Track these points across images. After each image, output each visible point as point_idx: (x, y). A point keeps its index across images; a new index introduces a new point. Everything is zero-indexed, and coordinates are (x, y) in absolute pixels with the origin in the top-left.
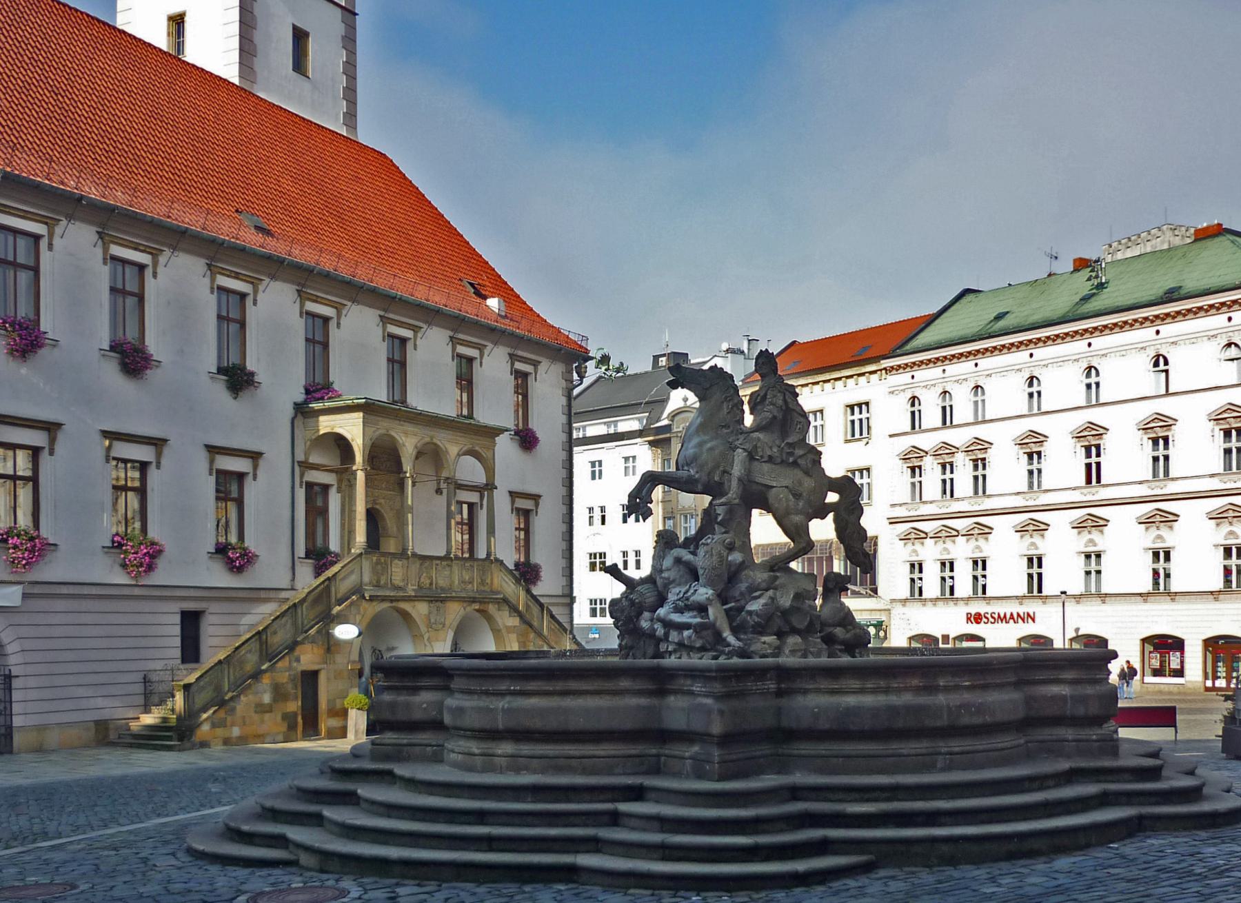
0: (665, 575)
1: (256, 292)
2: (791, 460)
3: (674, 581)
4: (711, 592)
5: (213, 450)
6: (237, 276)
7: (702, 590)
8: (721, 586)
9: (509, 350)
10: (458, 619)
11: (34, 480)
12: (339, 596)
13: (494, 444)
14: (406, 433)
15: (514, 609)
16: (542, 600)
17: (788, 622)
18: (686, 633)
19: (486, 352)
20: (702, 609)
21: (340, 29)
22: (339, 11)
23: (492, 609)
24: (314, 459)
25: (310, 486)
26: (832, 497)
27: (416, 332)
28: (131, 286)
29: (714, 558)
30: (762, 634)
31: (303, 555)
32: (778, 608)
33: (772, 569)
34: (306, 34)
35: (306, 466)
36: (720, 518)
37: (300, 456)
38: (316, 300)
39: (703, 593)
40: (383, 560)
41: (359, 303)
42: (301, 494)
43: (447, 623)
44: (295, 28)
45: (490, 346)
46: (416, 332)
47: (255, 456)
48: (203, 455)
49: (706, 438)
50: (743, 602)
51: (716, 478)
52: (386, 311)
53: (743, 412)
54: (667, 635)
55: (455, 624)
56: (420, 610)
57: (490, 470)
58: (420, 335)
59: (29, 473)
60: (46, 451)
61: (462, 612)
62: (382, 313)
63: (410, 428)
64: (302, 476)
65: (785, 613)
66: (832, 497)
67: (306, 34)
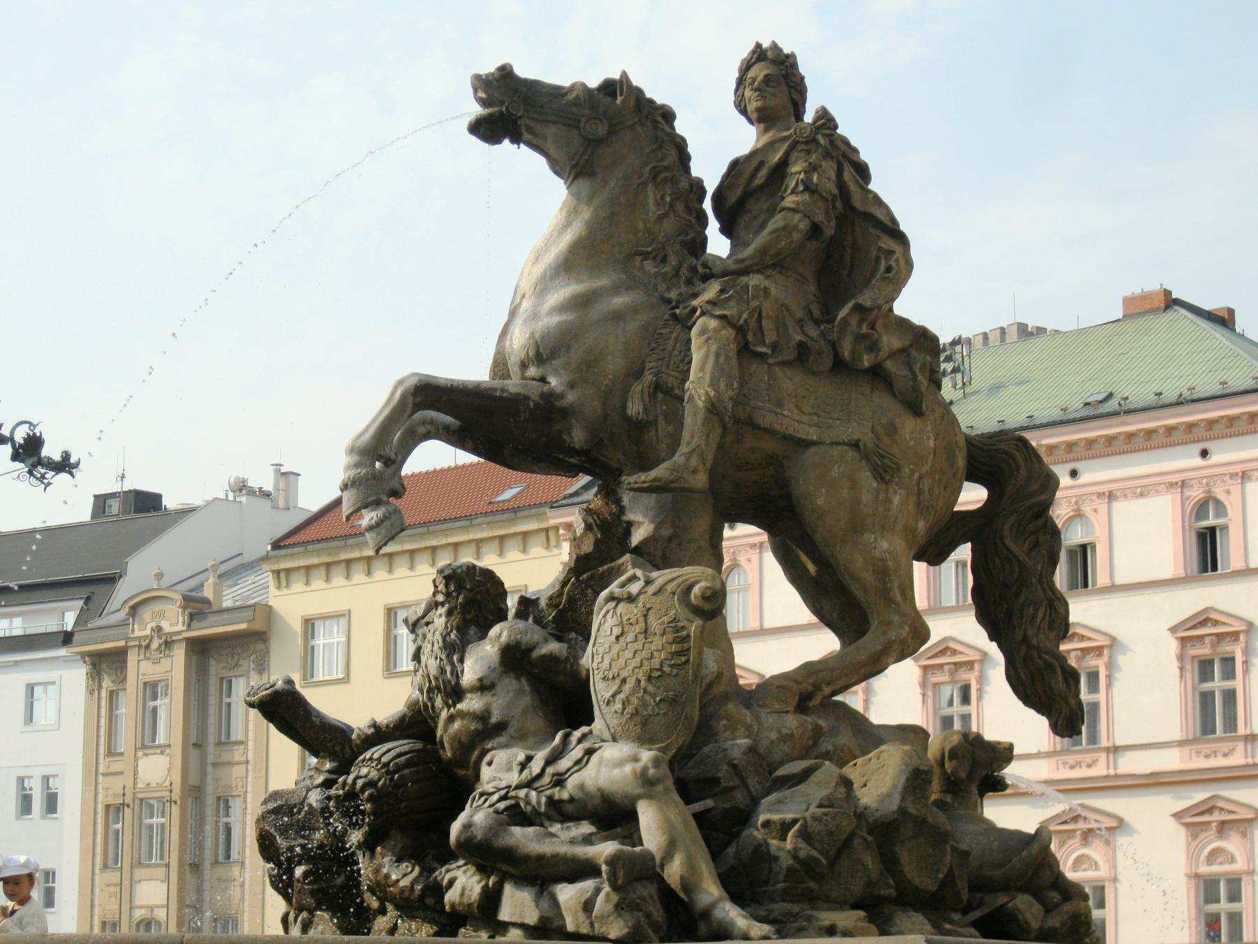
0: (472, 703)
2: (866, 362)
3: (501, 727)
4: (646, 755)
7: (611, 752)
8: (679, 739)
17: (890, 864)
18: (567, 894)
20: (614, 816)
26: (973, 496)
29: (658, 642)
30: (813, 900)
32: (861, 815)
33: (802, 707)
36: (637, 537)
39: (610, 760)
49: (602, 282)
50: (740, 799)
51: (635, 408)
53: (702, 220)
54: (491, 899)
65: (884, 831)
66: (973, 496)
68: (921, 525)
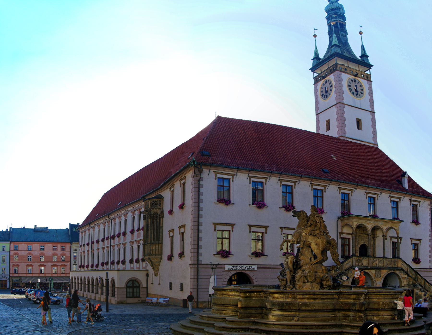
1: (325, 189)
6: (319, 185)
9: (409, 198)
10: (386, 275)
12: (345, 268)
14: (368, 224)
15: (406, 273)
16: (415, 269)
19: (401, 199)
21: (371, 117)
23: (397, 272)
24: (343, 231)
25: (343, 239)
27: (377, 196)
34: (361, 120)
35: (341, 233)
37: (339, 230)
38: (344, 189)
43: (382, 276)
44: (357, 119)
45: (402, 197)
46: (377, 196)
48: (280, 229)
55: (385, 276)
56: (372, 272)
57: (398, 233)
61: (387, 273)
63: (368, 222)
64: (340, 236)
67: (361, 120)
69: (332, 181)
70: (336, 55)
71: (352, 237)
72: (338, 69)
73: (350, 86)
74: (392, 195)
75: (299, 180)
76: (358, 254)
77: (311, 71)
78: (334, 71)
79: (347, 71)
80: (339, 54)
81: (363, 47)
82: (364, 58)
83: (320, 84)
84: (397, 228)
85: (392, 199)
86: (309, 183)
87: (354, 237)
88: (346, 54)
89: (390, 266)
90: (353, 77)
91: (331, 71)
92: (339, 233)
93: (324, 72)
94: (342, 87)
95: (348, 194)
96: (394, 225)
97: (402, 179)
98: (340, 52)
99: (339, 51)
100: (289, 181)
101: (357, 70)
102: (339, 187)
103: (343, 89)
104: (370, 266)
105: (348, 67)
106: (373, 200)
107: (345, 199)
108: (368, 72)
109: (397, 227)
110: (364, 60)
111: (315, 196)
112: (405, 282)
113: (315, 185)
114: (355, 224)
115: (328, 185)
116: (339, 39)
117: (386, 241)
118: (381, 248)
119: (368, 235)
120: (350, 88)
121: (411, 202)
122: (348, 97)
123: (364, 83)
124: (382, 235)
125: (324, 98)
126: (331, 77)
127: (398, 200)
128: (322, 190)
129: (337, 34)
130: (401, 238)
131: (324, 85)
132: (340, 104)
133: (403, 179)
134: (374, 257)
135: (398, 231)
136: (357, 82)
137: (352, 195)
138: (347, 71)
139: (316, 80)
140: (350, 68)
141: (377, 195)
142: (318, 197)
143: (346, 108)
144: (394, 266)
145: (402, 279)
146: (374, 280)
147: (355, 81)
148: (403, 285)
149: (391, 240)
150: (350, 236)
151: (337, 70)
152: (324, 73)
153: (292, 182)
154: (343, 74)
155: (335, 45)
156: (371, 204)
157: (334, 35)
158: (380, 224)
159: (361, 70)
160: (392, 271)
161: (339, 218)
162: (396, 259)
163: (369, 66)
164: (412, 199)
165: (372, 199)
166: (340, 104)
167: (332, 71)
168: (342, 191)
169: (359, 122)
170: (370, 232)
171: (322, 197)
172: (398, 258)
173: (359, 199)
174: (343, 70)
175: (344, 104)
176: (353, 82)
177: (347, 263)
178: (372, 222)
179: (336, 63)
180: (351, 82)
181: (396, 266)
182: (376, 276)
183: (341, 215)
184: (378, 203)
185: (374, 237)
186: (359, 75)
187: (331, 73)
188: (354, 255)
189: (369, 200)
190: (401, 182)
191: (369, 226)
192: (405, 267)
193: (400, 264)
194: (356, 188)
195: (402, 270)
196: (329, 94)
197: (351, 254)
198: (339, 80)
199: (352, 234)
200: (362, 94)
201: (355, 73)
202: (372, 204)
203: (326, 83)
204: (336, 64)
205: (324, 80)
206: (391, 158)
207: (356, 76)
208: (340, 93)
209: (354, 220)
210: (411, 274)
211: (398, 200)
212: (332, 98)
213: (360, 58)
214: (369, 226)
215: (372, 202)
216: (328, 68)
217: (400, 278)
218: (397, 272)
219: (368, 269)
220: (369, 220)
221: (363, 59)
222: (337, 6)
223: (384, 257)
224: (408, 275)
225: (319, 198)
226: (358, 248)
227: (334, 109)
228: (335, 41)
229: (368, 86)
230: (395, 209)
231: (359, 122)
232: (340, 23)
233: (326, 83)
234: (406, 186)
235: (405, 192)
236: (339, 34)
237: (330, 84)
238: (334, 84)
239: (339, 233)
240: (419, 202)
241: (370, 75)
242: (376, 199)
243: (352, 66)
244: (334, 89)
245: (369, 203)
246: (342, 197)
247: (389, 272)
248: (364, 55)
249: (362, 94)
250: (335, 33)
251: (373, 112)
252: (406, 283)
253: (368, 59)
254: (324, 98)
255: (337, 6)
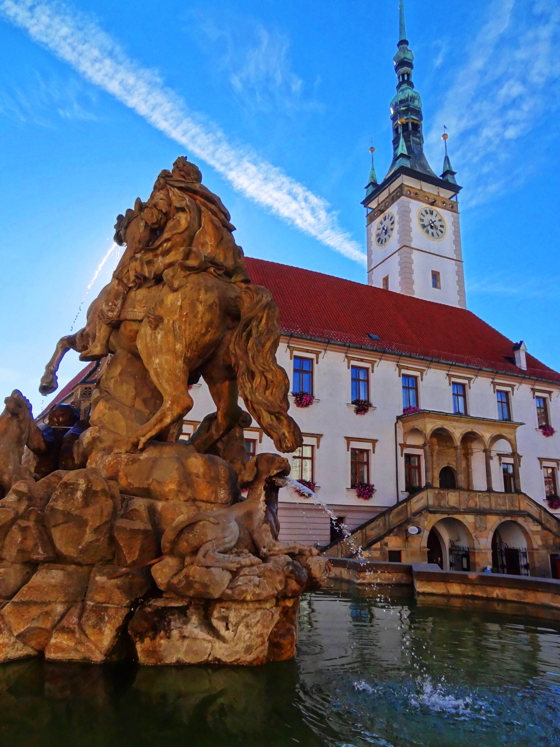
5: (349, 439)
6: (362, 360)
9: (530, 386)
11: (312, 459)
12: (413, 511)
13: (515, 432)
14: (455, 428)
15: (538, 522)
19: (515, 388)
22: (454, 261)
23: (520, 520)
28: (306, 368)
31: (404, 489)
34: (438, 273)
35: (404, 446)
37: (400, 440)
38: (408, 368)
40: (442, 492)
41: (430, 368)
42: (402, 461)
44: (432, 271)
45: (517, 384)
47: (374, 442)
52: (449, 371)
56: (469, 520)
57: (514, 446)
58: (472, 382)
59: (311, 456)
60: (258, 441)
61: (499, 522)
62: (447, 372)
63: (455, 424)
67: (438, 273)
68: (178, 346)
69: (384, 352)
70: (403, 170)
71: (425, 452)
72: (404, 193)
73: (423, 220)
74: (496, 381)
75: (325, 350)
76: (437, 484)
77: (363, 205)
78: (399, 197)
79: (419, 197)
80: (407, 168)
81: (447, 159)
82: (449, 177)
83: (376, 223)
84: (512, 437)
85: (498, 388)
86: (343, 355)
87: (429, 454)
88: (418, 169)
89: (503, 508)
90: (428, 206)
91: (393, 198)
92: (400, 444)
93: (382, 202)
94: (410, 221)
95: (416, 377)
96: (505, 431)
97: (514, 355)
98: (409, 166)
99: (407, 164)
100: (307, 351)
101: (435, 195)
102: (397, 365)
103: (412, 225)
104: (463, 507)
105: (421, 190)
106: (462, 390)
107: (410, 386)
108: (454, 199)
109: (511, 434)
110: (447, 180)
111: (355, 380)
112: (537, 542)
113: (354, 359)
114: (430, 426)
115: (378, 360)
116: (409, 148)
117: (491, 461)
118: (483, 474)
119: (456, 448)
120: (422, 223)
121: (534, 394)
122: (418, 237)
123: (447, 216)
124: (483, 448)
125: (382, 243)
126: (393, 210)
127: (508, 389)
128: (367, 369)
129: (407, 141)
130: (520, 457)
131: (381, 223)
132: (405, 247)
133: (516, 355)
134: (469, 489)
135: (513, 443)
136: (435, 213)
137: (422, 380)
138: (419, 197)
139: (371, 218)
140: (424, 192)
141: (469, 379)
142: (359, 380)
143: (415, 255)
144: (512, 509)
145: (530, 534)
146: (473, 535)
147: (432, 213)
148: (535, 546)
149: (500, 460)
150: (420, 452)
151: (403, 195)
152: (383, 204)
153: (312, 352)
154: (412, 200)
155: (402, 155)
156: (458, 395)
157: (402, 140)
158: (479, 430)
159: (441, 195)
160: (509, 519)
161: (398, 418)
162: (515, 495)
163: (456, 189)
164: (536, 387)
165: (460, 388)
166: (405, 247)
167: (393, 199)
168: (404, 371)
169: (435, 276)
170: (458, 443)
171: (367, 381)
172: (518, 492)
173: (436, 386)
174: (412, 195)
175: (413, 248)
176: (427, 213)
177: (417, 501)
178: (461, 425)
179: (402, 184)
180: (424, 213)
181: (517, 509)
182: (476, 528)
183: (402, 413)
184: (471, 393)
185: (467, 455)
186: (439, 202)
187: (394, 202)
188: (429, 486)
189: (454, 390)
190: (512, 360)
191: (457, 431)
192: (534, 511)
193: (524, 506)
194: (429, 367)
195: (530, 516)
196: (389, 236)
197: (423, 484)
198: (405, 213)
199: (423, 447)
200: (442, 232)
201: (431, 200)
202: (460, 395)
203: (385, 219)
204: (401, 186)
205: (382, 216)
206: (493, 327)
207: (432, 204)
208: (406, 232)
209: (427, 420)
210: (548, 525)
211: (508, 389)
212: (394, 241)
213: (441, 178)
214: (457, 431)
215: (460, 391)
216: (390, 195)
217: (526, 533)
218: (520, 520)
219: (459, 513)
220: (457, 421)
221: (446, 178)
222: (410, 94)
223: (490, 490)
224: (544, 528)
225: (361, 383)
226: (437, 474)
227: (396, 258)
228: (402, 149)
229: (452, 219)
230: (505, 405)
231: (435, 276)
232: (413, 123)
233: (385, 219)
234: (523, 364)
235: (521, 376)
236: (410, 141)
237: (391, 220)
238: (396, 218)
239: (400, 444)
240: (550, 393)
241: (457, 202)
242: (467, 387)
243: (429, 188)
244: (396, 227)
245: (453, 394)
246: (404, 382)
247: (503, 520)
248: (448, 172)
249: (442, 232)
250: (404, 137)
251: (459, 261)
252: (540, 543)
253: (454, 178)
254: (382, 243)
255: (410, 94)
